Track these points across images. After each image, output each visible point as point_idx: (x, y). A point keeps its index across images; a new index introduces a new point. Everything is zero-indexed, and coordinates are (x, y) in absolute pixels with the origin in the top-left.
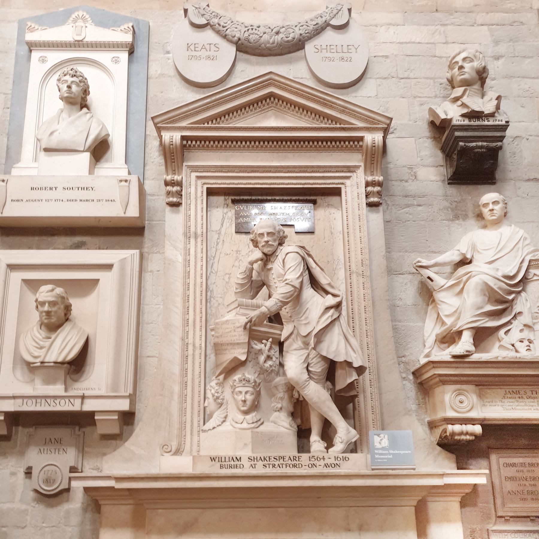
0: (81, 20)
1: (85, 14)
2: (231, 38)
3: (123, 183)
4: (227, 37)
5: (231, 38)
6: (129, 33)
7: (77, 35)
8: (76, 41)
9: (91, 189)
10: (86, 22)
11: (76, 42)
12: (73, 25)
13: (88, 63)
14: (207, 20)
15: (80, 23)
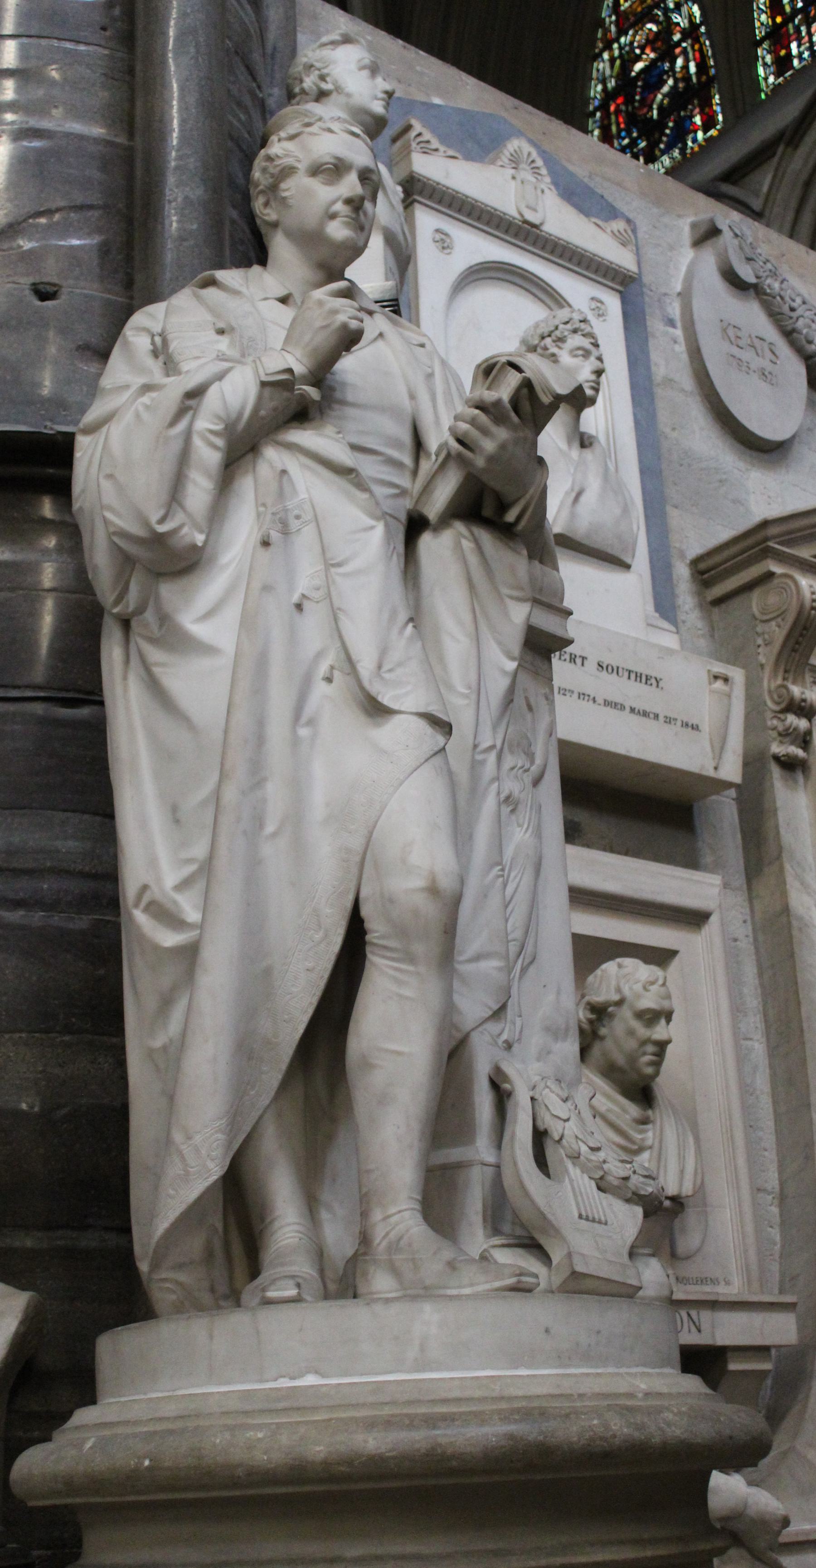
0: (528, 168)
1: (534, 154)
2: (804, 342)
3: (719, 684)
4: (795, 335)
5: (804, 342)
6: (630, 247)
7: (528, 207)
8: (526, 222)
9: (653, 681)
10: (539, 177)
11: (526, 226)
12: (513, 171)
13: (534, 290)
14: (758, 277)
15: (526, 174)
